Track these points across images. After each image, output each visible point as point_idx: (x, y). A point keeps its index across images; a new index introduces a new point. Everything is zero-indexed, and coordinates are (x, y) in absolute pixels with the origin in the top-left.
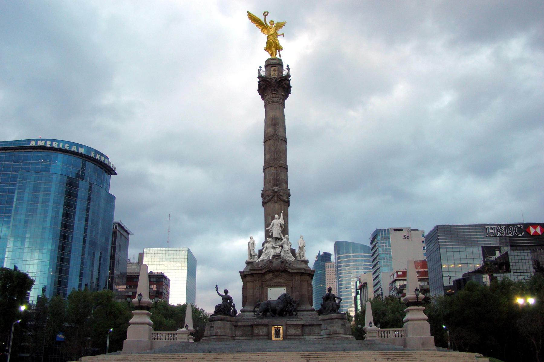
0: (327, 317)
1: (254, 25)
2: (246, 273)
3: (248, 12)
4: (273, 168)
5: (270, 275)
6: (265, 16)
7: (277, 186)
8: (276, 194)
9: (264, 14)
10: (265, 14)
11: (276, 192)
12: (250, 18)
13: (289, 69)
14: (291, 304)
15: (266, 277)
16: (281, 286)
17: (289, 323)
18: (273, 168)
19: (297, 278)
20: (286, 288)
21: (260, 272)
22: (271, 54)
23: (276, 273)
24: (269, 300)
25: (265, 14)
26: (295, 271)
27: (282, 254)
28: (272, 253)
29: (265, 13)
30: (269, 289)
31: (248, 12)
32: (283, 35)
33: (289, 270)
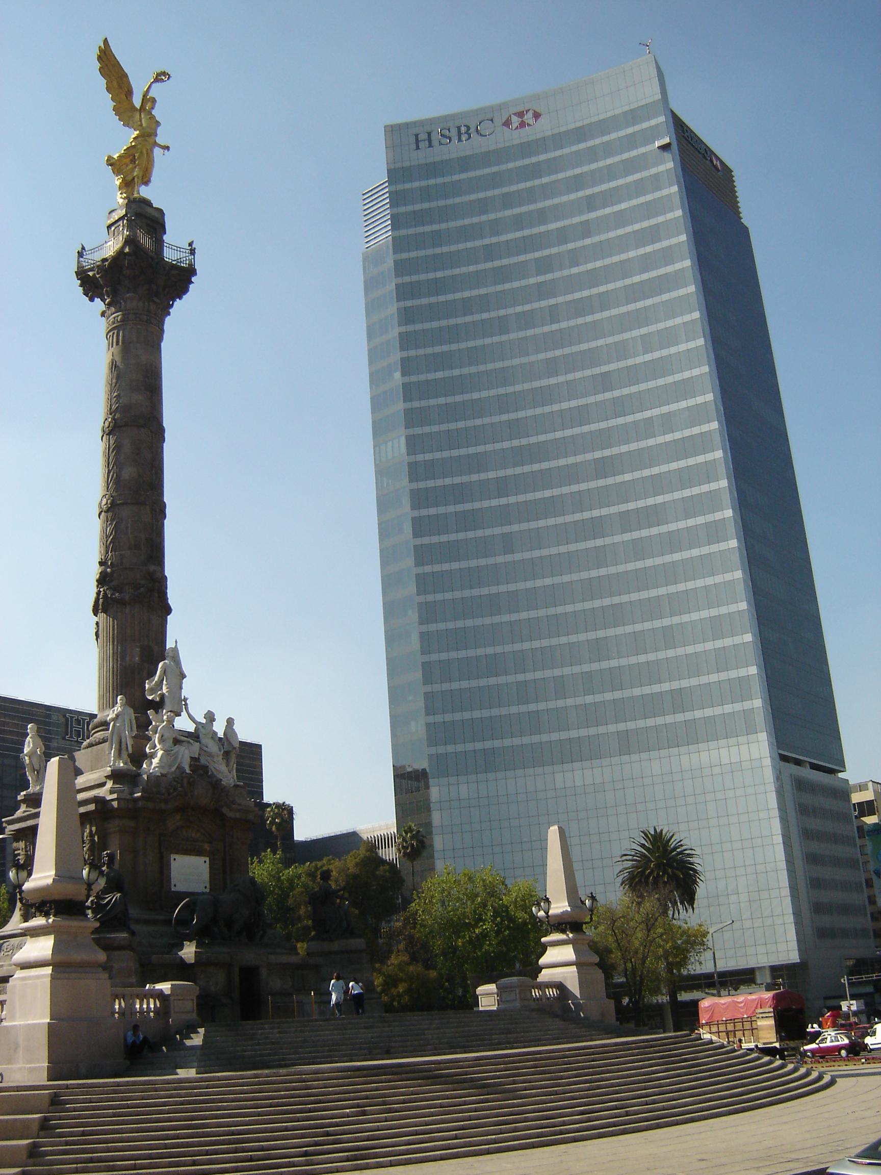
0: (336, 946)
1: (103, 82)
3: (106, 41)
6: (157, 80)
9: (158, 75)
10: (161, 76)
13: (193, 252)
16: (199, 853)
17: (272, 958)
20: (207, 859)
21: (163, 806)
22: (128, 185)
24: (173, 889)
25: (161, 76)
26: (238, 815)
27: (203, 761)
28: (185, 754)
29: (164, 74)
30: (173, 856)
31: (106, 41)
32: (167, 148)
33: (225, 810)
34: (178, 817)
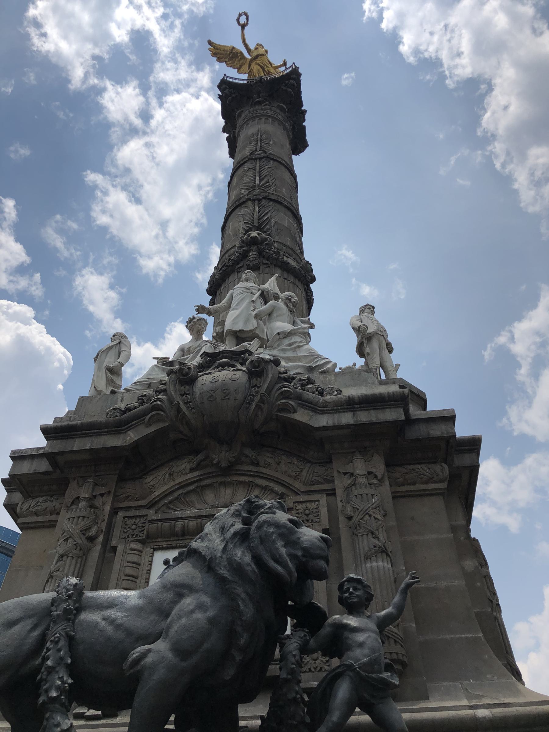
2: (26, 468)
3: (210, 43)
4: (250, 203)
5: (183, 471)
6: (243, 26)
7: (258, 228)
8: (255, 248)
11: (254, 242)
12: (214, 55)
14: (311, 618)
15: (150, 480)
18: (250, 203)
19: (359, 466)
23: (222, 456)
26: (347, 418)
29: (240, 15)
31: (210, 43)
33: (301, 416)
34: (185, 465)
